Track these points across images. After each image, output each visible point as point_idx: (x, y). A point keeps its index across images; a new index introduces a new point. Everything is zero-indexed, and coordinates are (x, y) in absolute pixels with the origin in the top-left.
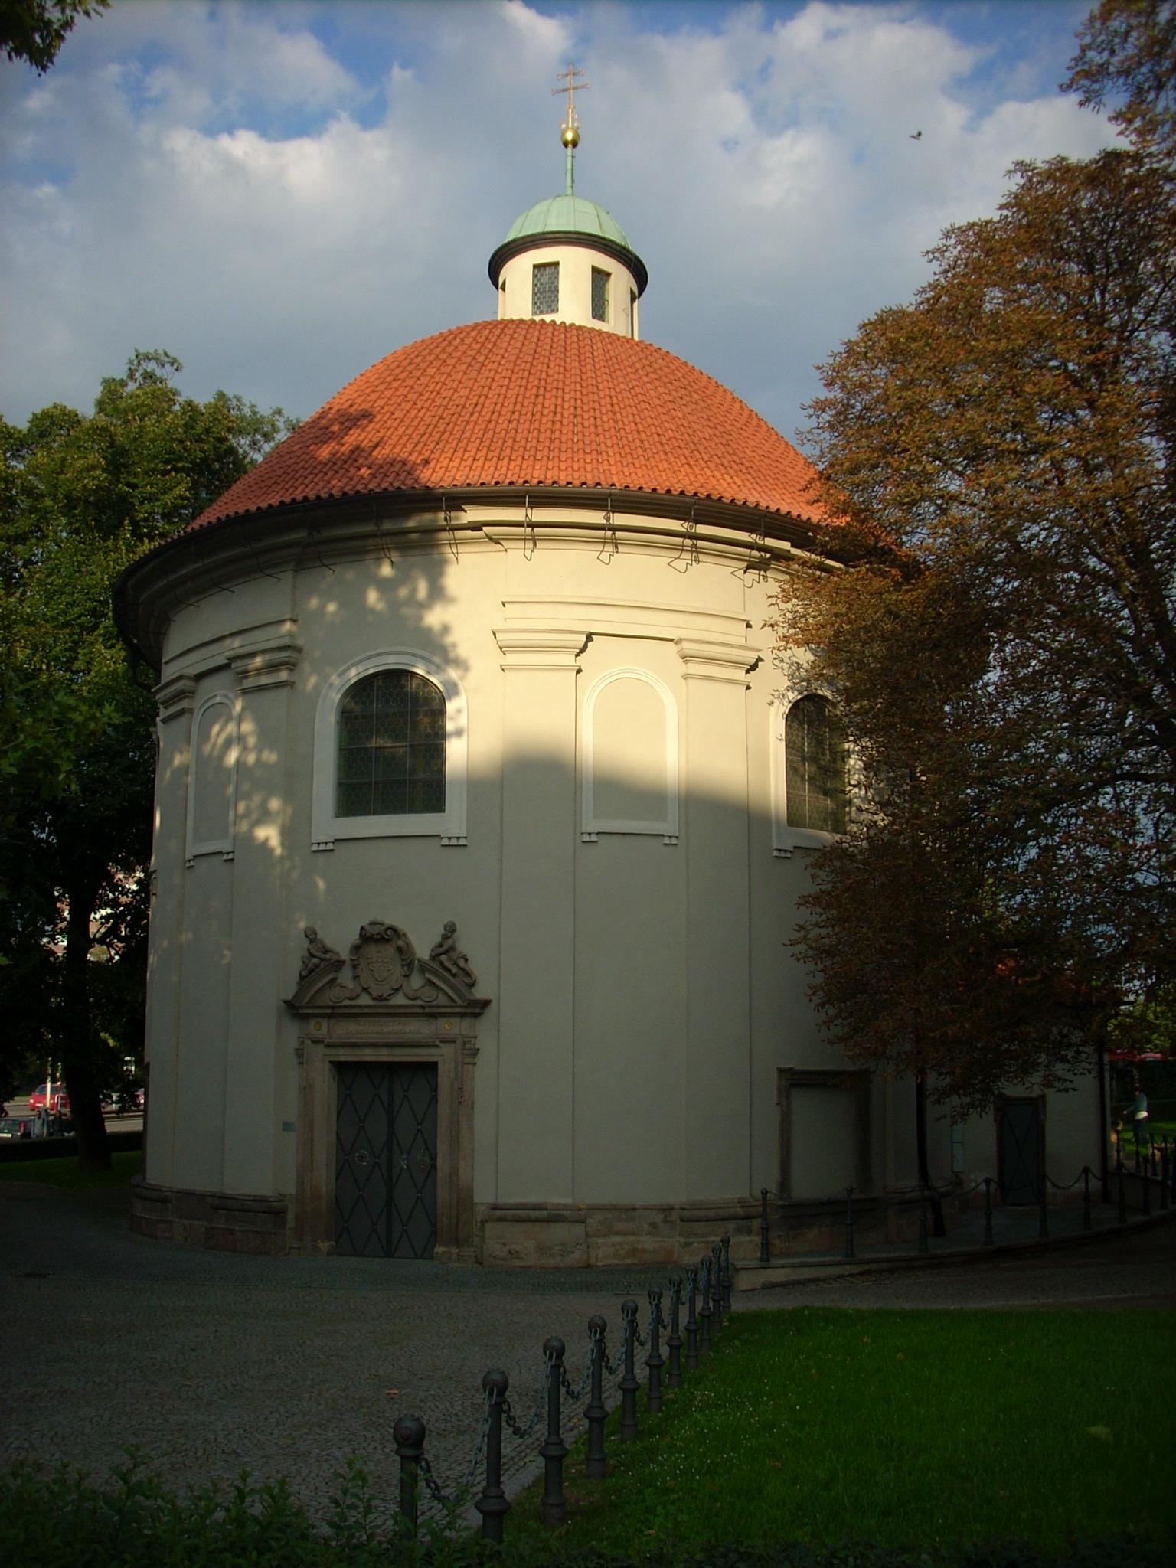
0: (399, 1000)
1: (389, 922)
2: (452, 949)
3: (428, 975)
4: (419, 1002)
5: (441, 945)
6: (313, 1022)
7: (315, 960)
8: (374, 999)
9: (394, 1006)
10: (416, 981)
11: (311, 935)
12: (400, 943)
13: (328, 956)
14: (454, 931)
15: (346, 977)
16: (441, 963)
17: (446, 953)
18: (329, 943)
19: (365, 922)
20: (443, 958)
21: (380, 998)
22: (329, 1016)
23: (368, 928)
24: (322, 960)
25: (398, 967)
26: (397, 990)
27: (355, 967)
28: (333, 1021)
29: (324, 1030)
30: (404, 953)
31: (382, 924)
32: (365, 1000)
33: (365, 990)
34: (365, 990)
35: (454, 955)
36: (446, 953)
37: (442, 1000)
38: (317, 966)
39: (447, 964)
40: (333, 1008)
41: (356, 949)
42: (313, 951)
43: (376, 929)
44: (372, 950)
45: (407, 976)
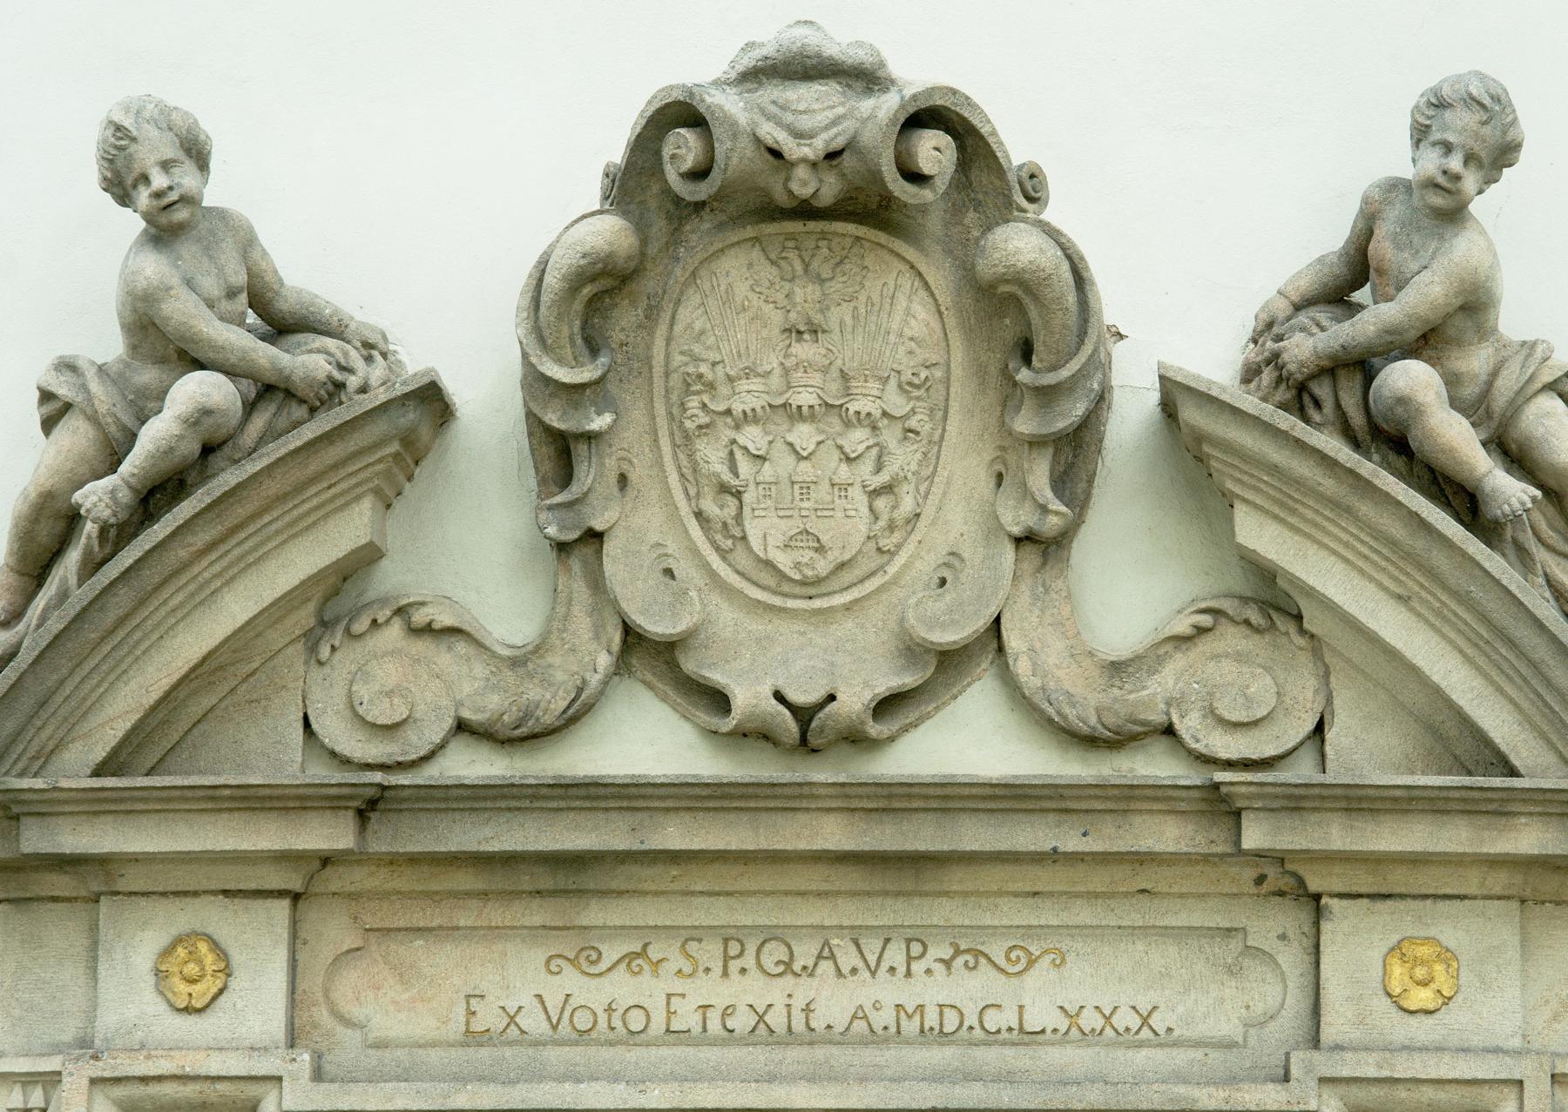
0: (969, 739)
1: (916, 72)
2: (1472, 306)
3: (1258, 534)
4: (1153, 766)
5: (1351, 277)
6: (138, 943)
7: (197, 390)
8: (756, 735)
9: (949, 798)
10: (1129, 584)
11: (155, 180)
12: (1016, 245)
13: (307, 361)
14: (1499, 156)
15: (473, 549)
16: (1393, 440)
17: (1426, 341)
18: (301, 275)
19: (701, 63)
20: (1410, 378)
21: (809, 731)
22: (302, 887)
23: (730, 105)
24: (269, 391)
25: (964, 466)
26: (949, 664)
27: (559, 453)
28: (333, 931)
29: (257, 1004)
30: (1029, 334)
31: (864, 77)
32: (644, 740)
33: (646, 654)
34: (646, 654)
35: (1475, 361)
36: (1426, 341)
37: (1367, 749)
38: (211, 447)
39: (1457, 438)
40: (369, 807)
41: (593, 304)
42: (189, 313)
43: (820, 113)
44: (732, 309)
45: (1042, 548)
